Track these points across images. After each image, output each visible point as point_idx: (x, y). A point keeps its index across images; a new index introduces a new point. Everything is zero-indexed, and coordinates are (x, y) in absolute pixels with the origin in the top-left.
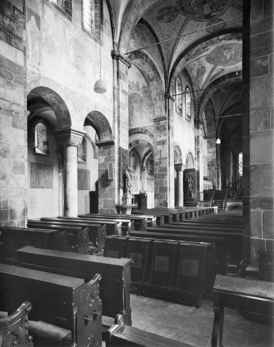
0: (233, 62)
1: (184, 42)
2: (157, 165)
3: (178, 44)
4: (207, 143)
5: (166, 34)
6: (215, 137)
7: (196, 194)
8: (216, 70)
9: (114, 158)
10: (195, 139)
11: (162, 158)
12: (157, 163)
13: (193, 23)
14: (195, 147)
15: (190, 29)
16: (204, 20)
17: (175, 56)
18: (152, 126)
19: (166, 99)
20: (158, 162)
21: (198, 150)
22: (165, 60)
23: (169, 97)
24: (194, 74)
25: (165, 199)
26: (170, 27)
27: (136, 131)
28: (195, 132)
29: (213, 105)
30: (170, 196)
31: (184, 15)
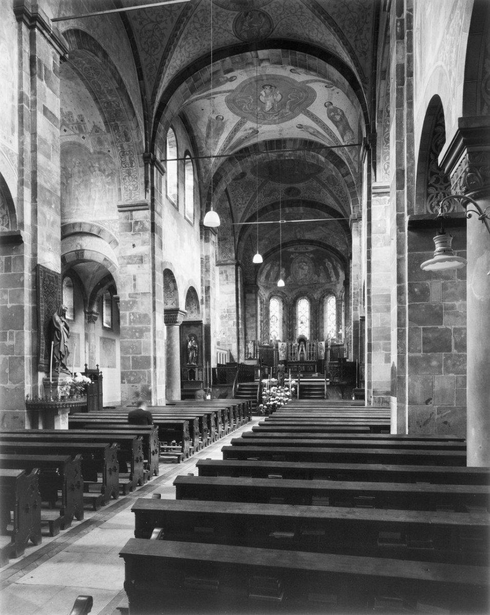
0: (275, 118)
1: (187, 46)
2: (127, 309)
3: (175, 47)
4: (220, 274)
5: (149, 18)
6: (232, 264)
7: (204, 372)
8: (242, 128)
9: (21, 280)
10: (202, 262)
11: (137, 294)
12: (127, 303)
14: (202, 277)
15: (202, 20)
17: (166, 75)
18: (115, 221)
19: (146, 165)
20: (130, 301)
21: (207, 285)
22: (145, 78)
23: (154, 162)
24: (202, 129)
25: (146, 383)
27: (77, 230)
28: (201, 247)
29: (232, 202)
30: (156, 375)
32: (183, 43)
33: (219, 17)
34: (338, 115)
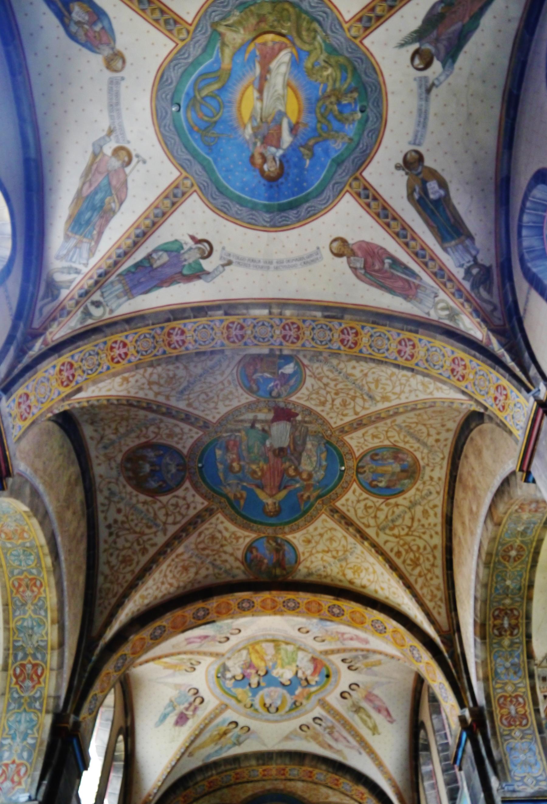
1: (389, 388)
13: (332, 415)
16: (298, 410)
26: (402, 437)
31: (345, 444)
32: (393, 397)
33: (323, 399)
34: (79, 23)
